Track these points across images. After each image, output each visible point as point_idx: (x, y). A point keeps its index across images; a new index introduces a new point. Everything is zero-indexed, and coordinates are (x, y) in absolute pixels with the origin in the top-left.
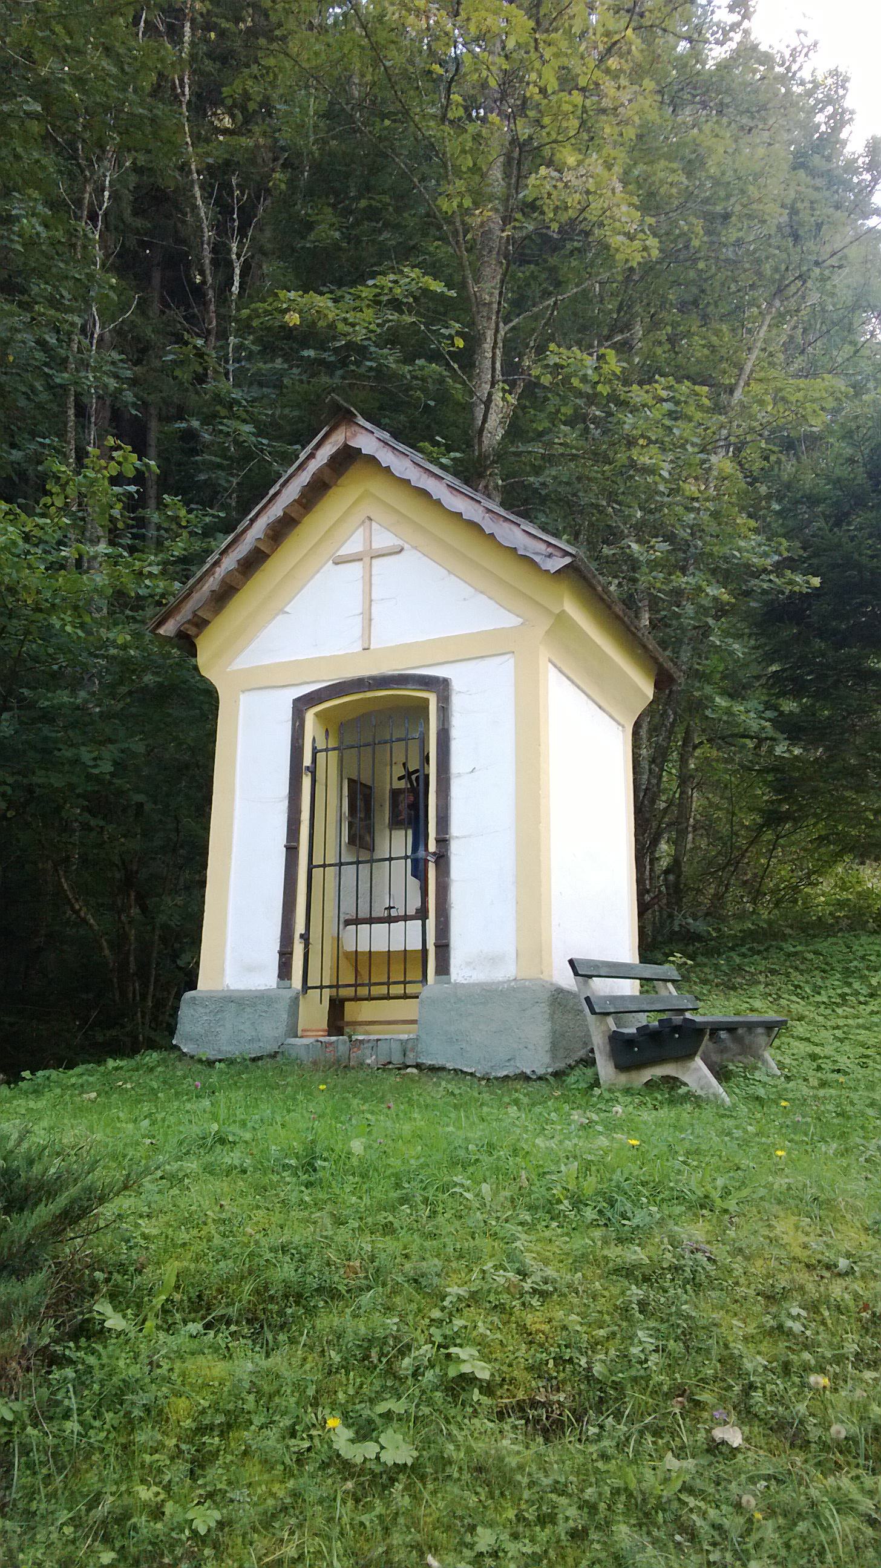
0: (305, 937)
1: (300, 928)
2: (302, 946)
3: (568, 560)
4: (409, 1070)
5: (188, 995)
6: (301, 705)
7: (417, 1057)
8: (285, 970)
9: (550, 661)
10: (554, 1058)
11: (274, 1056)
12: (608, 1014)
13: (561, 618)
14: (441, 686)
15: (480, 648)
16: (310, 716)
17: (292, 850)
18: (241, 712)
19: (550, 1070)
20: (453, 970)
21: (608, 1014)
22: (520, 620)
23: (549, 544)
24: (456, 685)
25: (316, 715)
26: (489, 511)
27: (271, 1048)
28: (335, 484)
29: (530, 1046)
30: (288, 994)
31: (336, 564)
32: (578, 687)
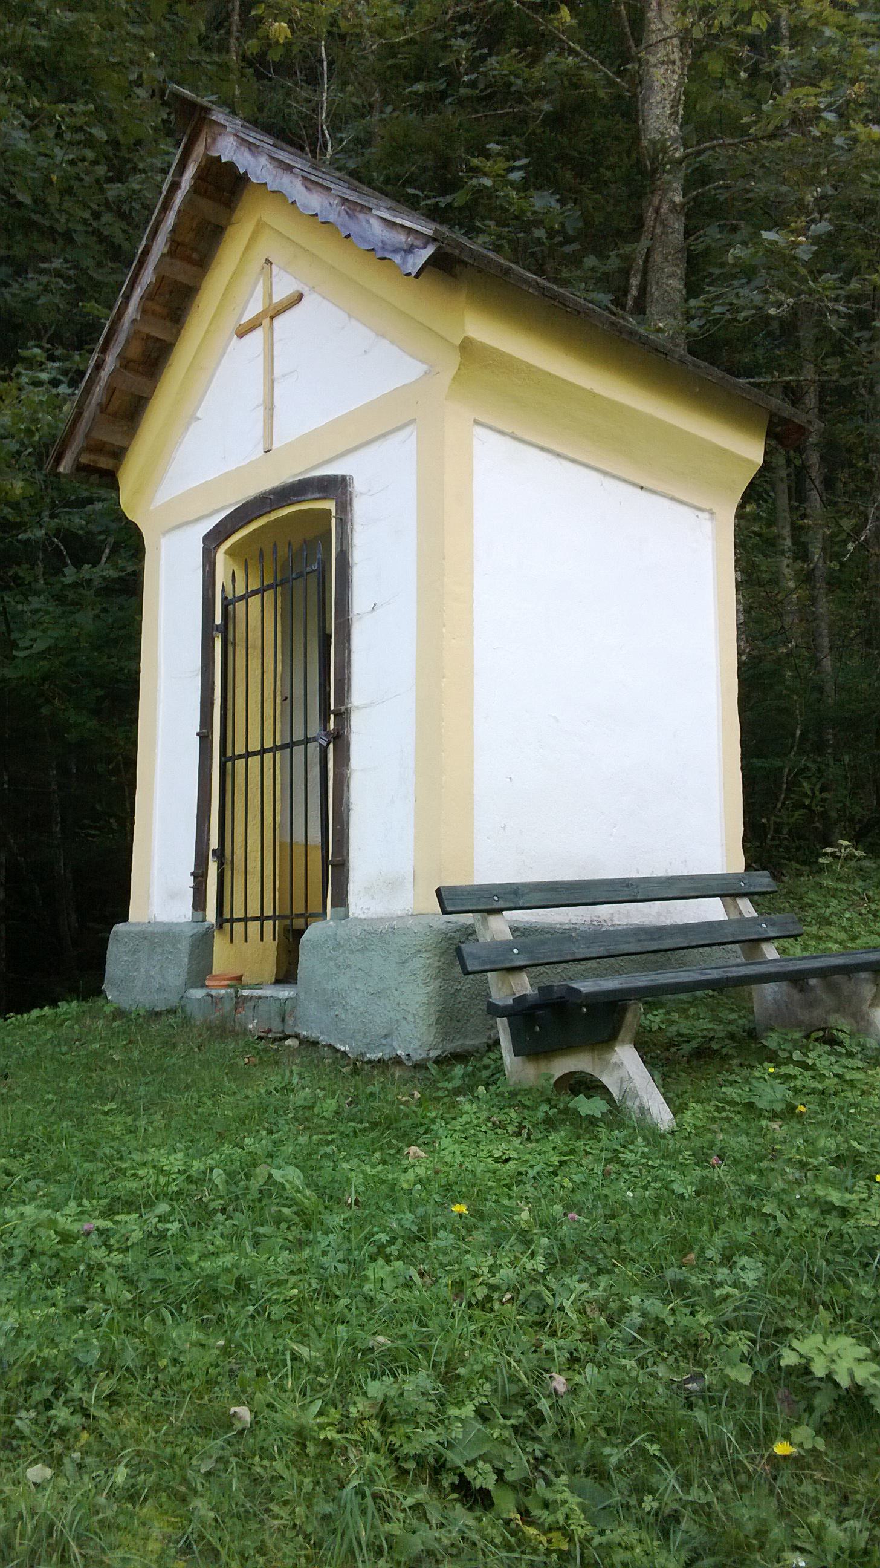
0: (220, 854)
1: (214, 844)
2: (215, 865)
3: (429, 251)
4: (288, 1042)
5: (119, 927)
6: (214, 539)
7: (295, 1024)
8: (199, 902)
9: (477, 422)
10: (445, 1036)
11: (173, 1011)
12: (520, 969)
13: (467, 348)
14: (336, 487)
15: (375, 425)
16: (221, 556)
17: (205, 738)
18: (163, 562)
19: (433, 1054)
20: (352, 899)
21: (520, 969)
22: (425, 367)
23: (409, 231)
24: (358, 486)
25: (227, 552)
26: (344, 201)
27: (173, 1001)
28: (229, 223)
29: (410, 1018)
30: (201, 928)
31: (240, 336)
32: (573, 461)
